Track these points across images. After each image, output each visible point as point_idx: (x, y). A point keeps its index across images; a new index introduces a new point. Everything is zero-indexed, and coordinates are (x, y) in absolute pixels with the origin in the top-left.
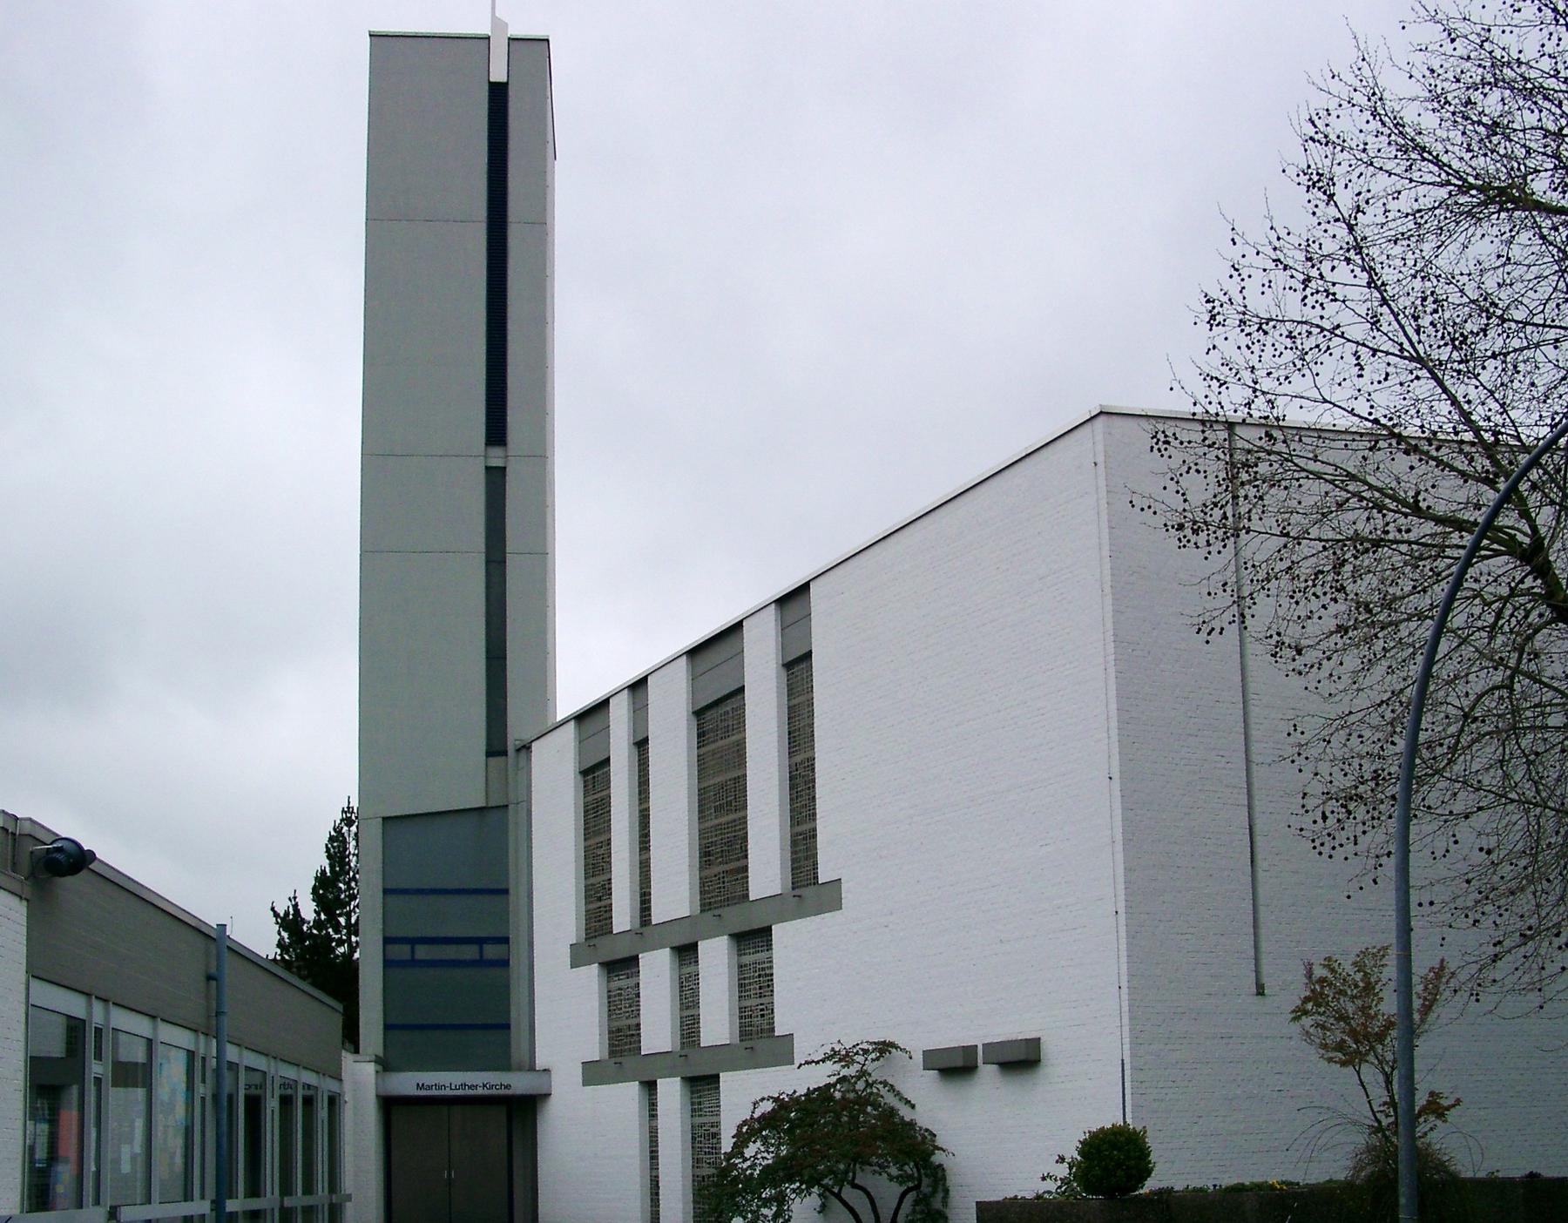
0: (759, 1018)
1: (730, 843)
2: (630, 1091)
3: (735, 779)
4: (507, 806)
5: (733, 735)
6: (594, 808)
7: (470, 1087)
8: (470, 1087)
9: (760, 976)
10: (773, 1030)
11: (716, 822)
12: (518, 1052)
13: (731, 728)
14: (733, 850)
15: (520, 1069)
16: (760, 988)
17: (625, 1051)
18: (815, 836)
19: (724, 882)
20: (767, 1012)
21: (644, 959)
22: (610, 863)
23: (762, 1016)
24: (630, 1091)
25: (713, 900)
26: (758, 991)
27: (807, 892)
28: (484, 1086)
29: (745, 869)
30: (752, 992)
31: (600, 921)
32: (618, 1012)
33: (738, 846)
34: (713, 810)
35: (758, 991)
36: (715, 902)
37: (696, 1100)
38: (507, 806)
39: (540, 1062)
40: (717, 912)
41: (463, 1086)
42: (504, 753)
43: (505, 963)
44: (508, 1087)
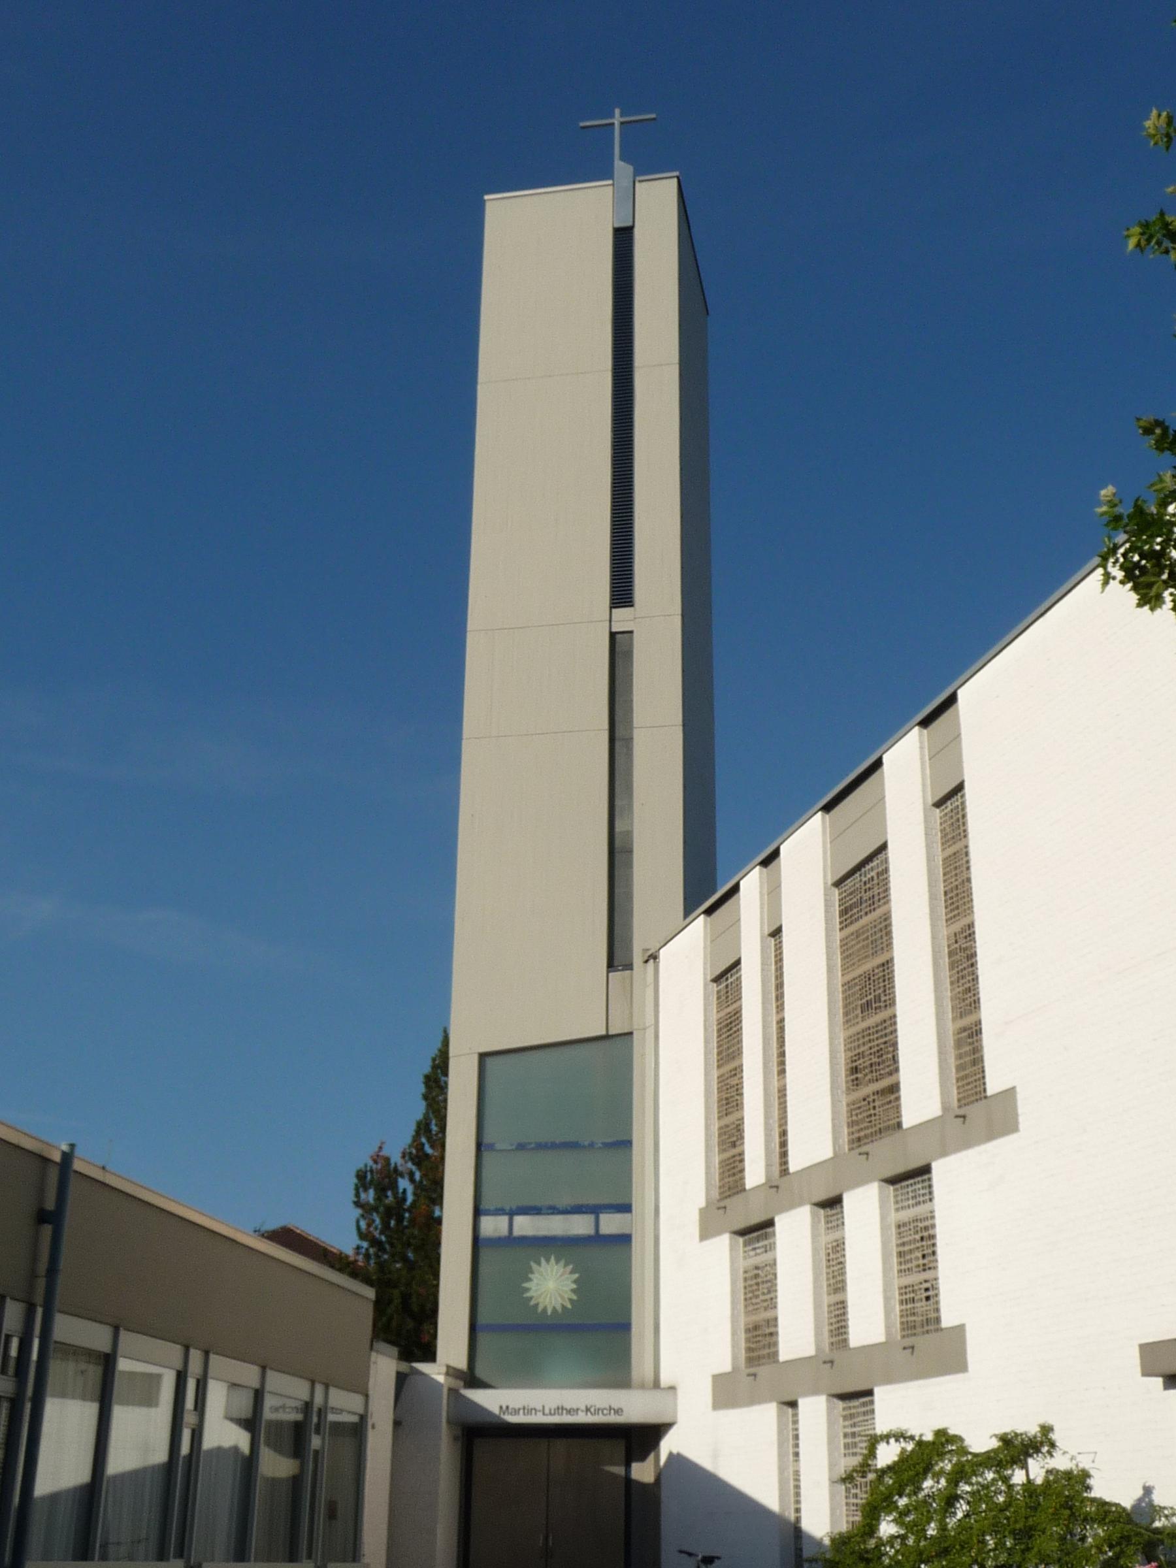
0: (924, 1303)
1: (879, 1053)
2: (767, 1414)
3: (883, 965)
4: (631, 1033)
5: (879, 906)
6: (727, 1025)
7: (569, 1412)
8: (569, 1412)
9: (922, 1239)
10: (938, 1320)
11: (864, 1025)
12: (641, 1366)
13: (876, 898)
14: (883, 1062)
15: (642, 1387)
16: (924, 1256)
17: (764, 1357)
18: (979, 1032)
19: (874, 1108)
20: (930, 1294)
21: (782, 1223)
22: (742, 1094)
23: (928, 1298)
24: (767, 1414)
25: (862, 1134)
26: (921, 1262)
27: (975, 1111)
28: (588, 1410)
29: (894, 1089)
30: (915, 1263)
31: (734, 1174)
32: (754, 1301)
33: (890, 1056)
34: (859, 1011)
35: (921, 1262)
36: (866, 1136)
37: (849, 1430)
38: (631, 1033)
39: (665, 1379)
40: (864, 1149)
41: (560, 1410)
42: (629, 966)
43: (624, 1240)
44: (618, 1411)
